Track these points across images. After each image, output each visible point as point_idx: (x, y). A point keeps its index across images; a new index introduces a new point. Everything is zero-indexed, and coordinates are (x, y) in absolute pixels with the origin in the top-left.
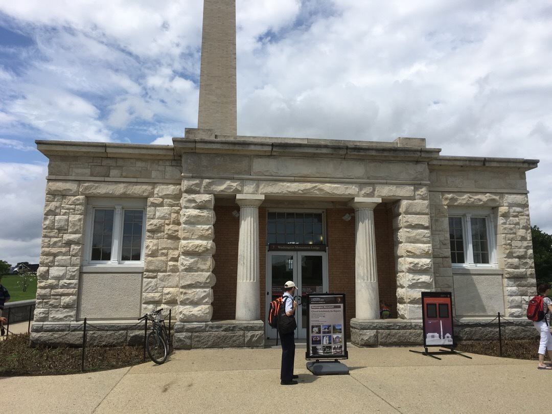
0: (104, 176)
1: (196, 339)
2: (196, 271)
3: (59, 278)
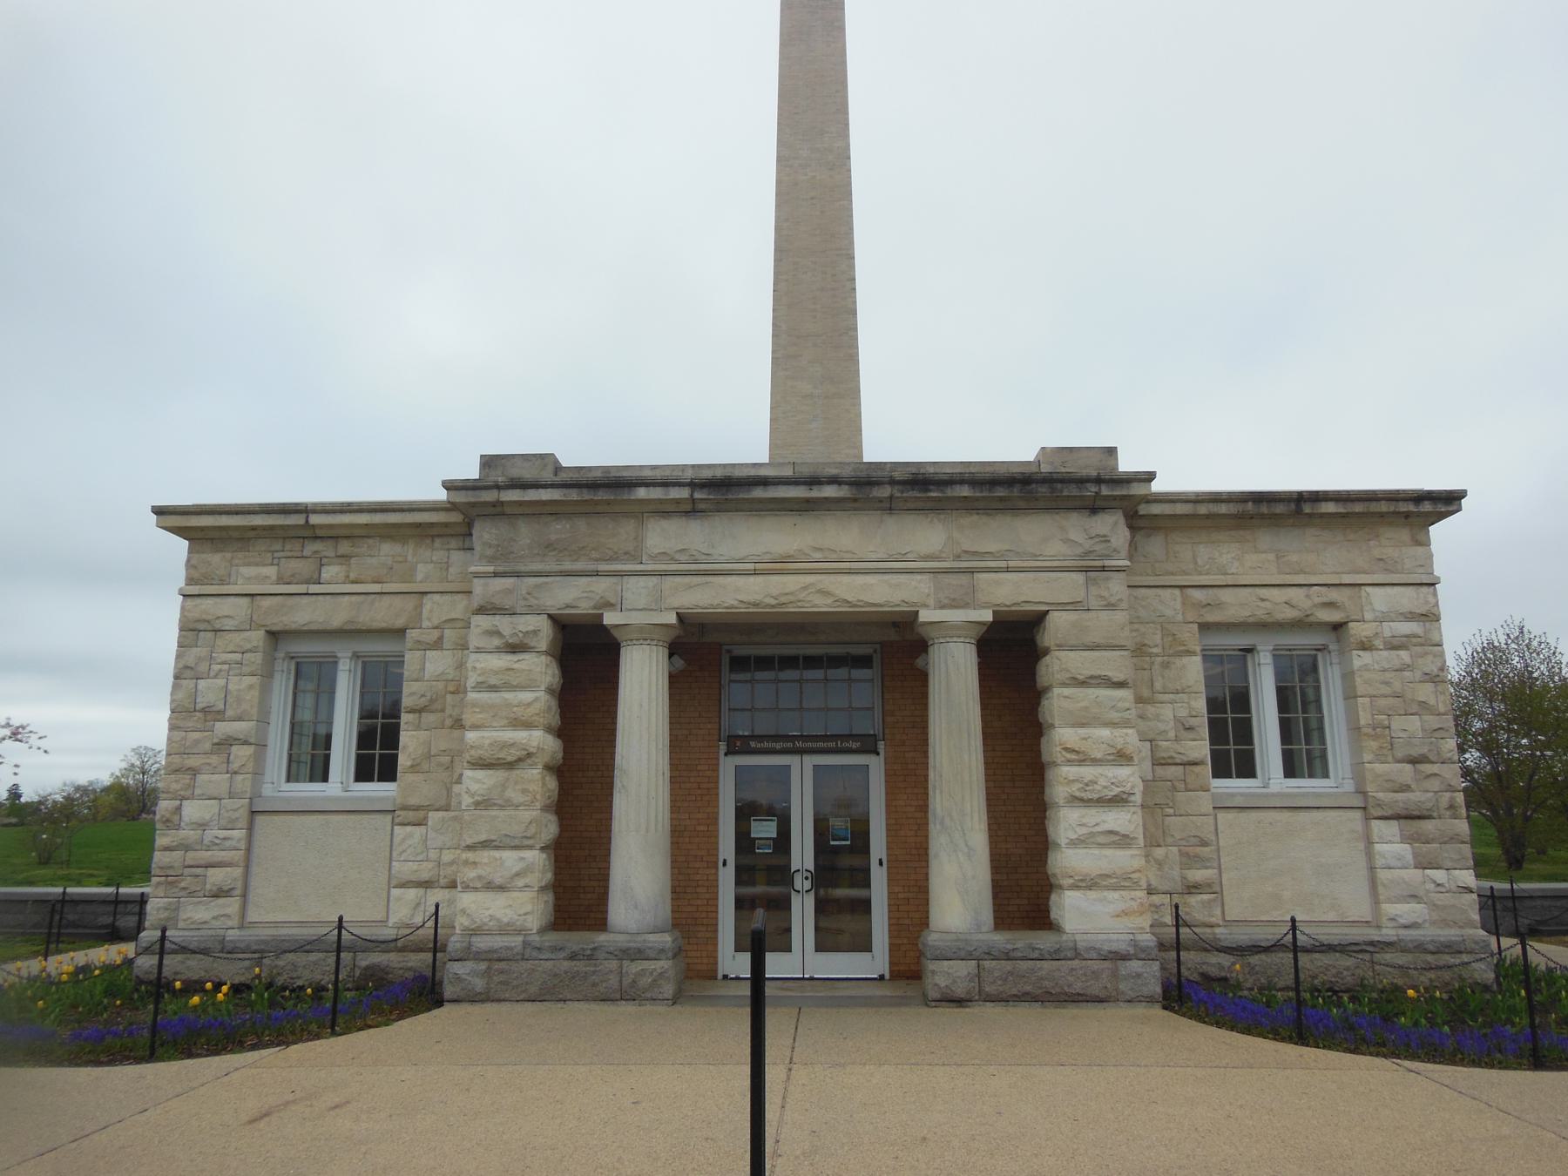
0: (308, 582)
1: (509, 980)
2: (502, 807)
3: (202, 826)
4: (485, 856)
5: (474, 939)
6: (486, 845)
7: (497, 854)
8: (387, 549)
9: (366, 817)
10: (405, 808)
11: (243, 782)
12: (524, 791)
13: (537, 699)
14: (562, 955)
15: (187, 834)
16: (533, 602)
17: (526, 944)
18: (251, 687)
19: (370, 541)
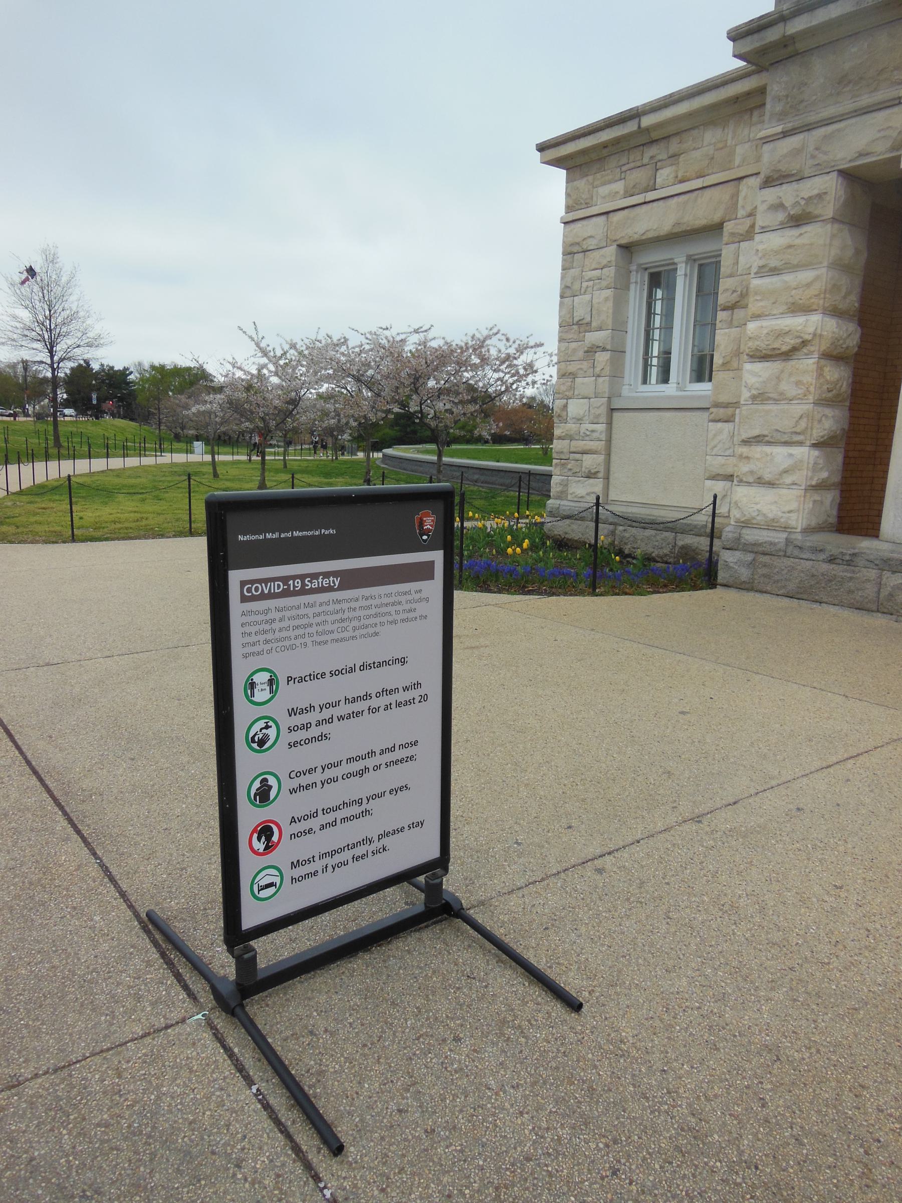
0: (646, 190)
1: (773, 573)
2: (776, 401)
3: (579, 420)
4: (757, 451)
5: (744, 531)
6: (758, 440)
7: (768, 449)
8: (710, 136)
9: (688, 414)
10: (717, 405)
11: (604, 384)
12: (798, 383)
13: (817, 278)
14: (822, 556)
15: (571, 427)
16: (822, 158)
17: (788, 541)
18: (607, 299)
19: (695, 133)
